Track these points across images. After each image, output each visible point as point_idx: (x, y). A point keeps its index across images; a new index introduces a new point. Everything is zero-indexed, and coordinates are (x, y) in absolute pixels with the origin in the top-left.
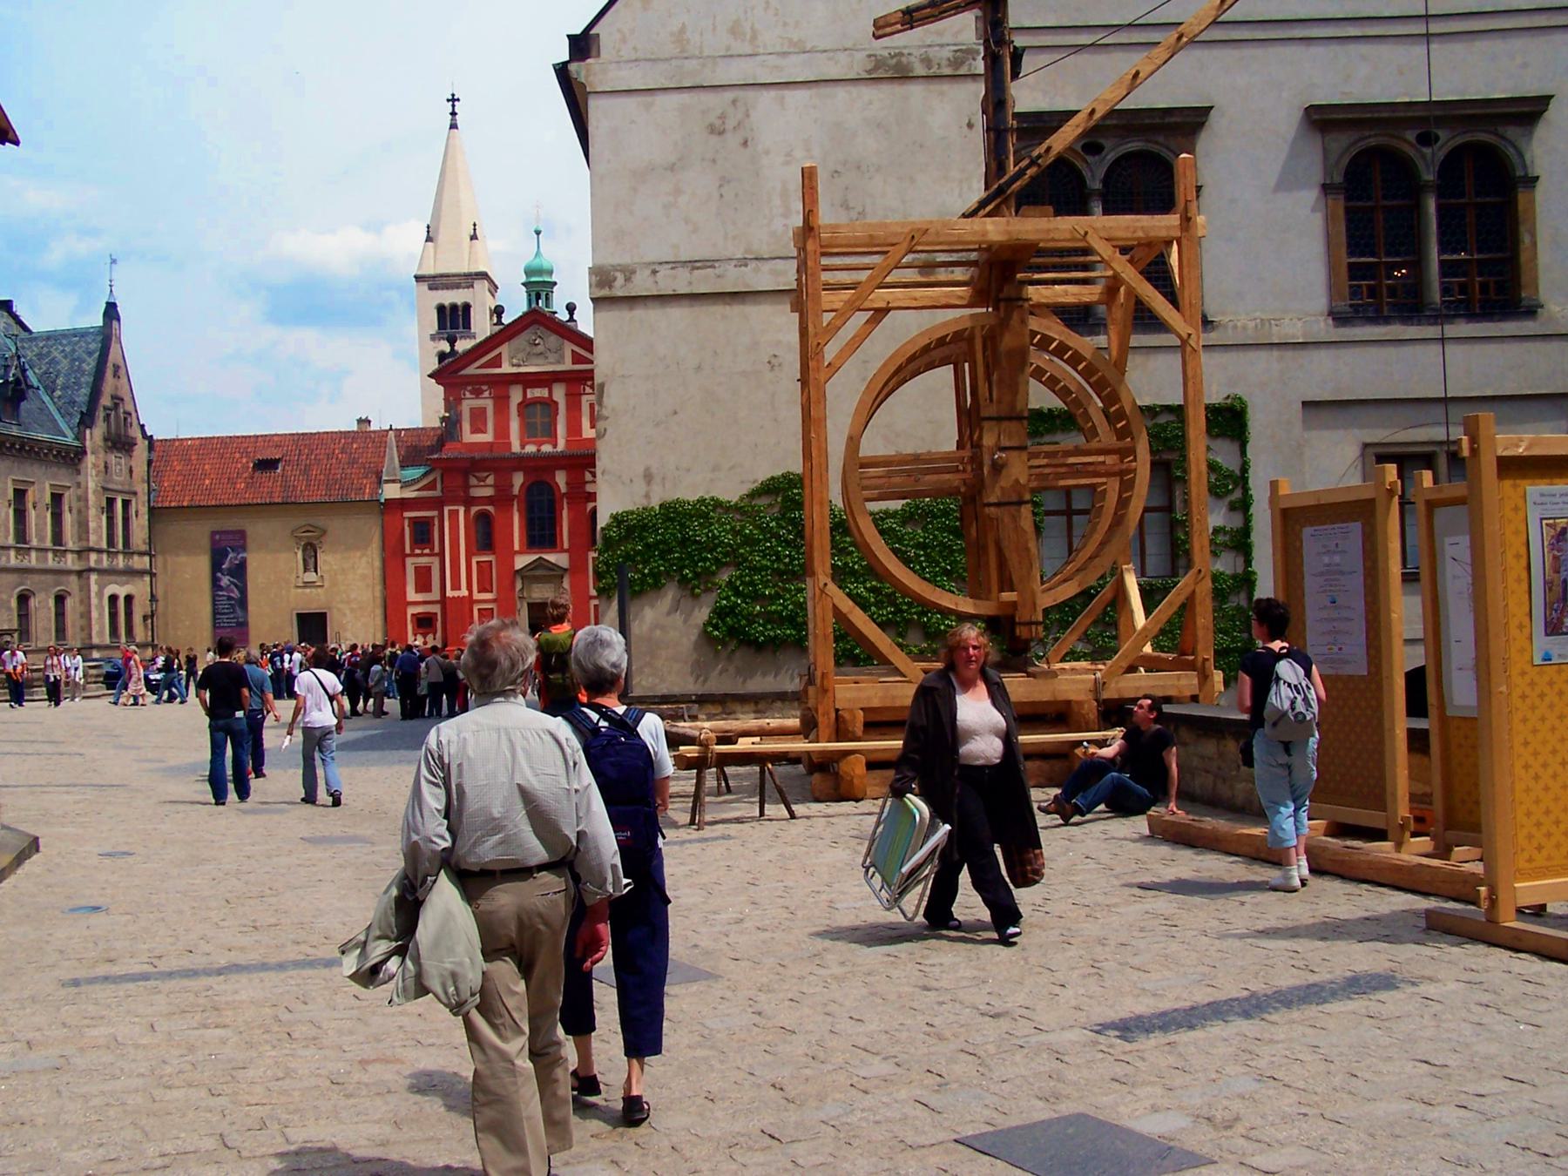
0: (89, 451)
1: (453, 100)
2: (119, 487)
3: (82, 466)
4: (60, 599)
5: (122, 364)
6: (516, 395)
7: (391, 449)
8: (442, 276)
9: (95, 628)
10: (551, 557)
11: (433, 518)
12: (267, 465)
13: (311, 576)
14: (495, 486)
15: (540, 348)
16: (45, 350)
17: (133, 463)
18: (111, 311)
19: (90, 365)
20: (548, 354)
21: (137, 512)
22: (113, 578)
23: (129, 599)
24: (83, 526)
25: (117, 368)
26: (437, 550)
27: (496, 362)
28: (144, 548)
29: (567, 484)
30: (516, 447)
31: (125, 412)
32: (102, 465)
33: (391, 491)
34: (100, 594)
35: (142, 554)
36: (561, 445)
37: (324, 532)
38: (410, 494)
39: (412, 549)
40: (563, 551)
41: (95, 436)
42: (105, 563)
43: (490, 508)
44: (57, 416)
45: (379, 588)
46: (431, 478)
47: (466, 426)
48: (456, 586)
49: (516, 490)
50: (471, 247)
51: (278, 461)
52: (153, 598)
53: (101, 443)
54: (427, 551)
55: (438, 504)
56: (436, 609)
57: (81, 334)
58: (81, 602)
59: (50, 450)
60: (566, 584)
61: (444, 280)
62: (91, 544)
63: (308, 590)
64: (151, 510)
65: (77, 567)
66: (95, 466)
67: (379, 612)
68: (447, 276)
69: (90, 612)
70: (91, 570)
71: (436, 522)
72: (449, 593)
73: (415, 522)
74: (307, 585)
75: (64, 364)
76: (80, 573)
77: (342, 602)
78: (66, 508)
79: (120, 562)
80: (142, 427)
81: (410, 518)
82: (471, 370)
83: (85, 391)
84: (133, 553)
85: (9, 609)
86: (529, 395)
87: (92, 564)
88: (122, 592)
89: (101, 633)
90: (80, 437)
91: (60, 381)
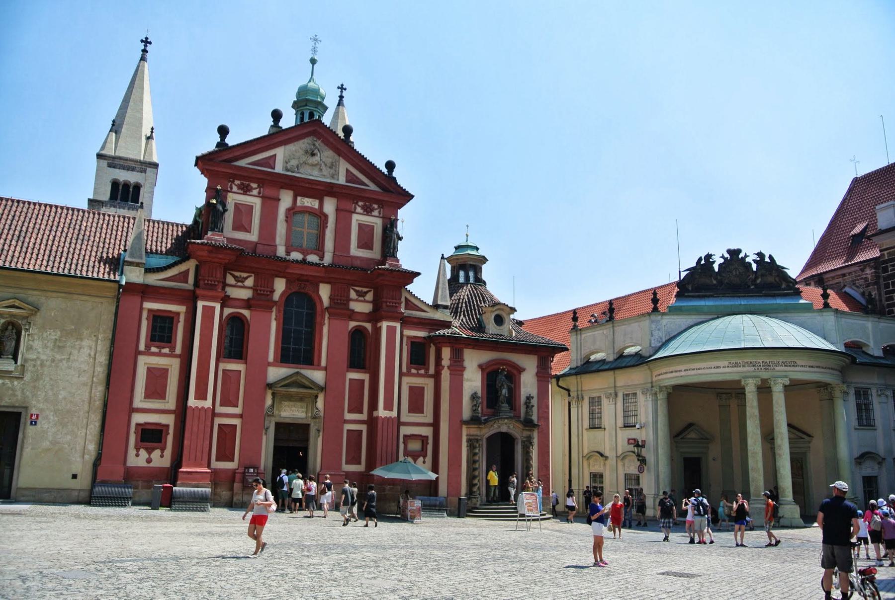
1: (146, 42)
6: (286, 199)
8: (120, 158)
11: (178, 314)
14: (254, 289)
20: (323, 167)
26: (178, 350)
29: (331, 298)
37: (36, 309)
38: (153, 279)
39: (148, 347)
40: (318, 367)
43: (246, 313)
46: (182, 268)
47: (229, 217)
48: (201, 395)
49: (276, 296)
50: (147, 144)
56: (169, 420)
60: (320, 403)
61: (122, 162)
68: (126, 160)
71: (182, 318)
72: (192, 402)
77: (46, 400)
81: (150, 311)
82: (243, 163)
86: (299, 203)
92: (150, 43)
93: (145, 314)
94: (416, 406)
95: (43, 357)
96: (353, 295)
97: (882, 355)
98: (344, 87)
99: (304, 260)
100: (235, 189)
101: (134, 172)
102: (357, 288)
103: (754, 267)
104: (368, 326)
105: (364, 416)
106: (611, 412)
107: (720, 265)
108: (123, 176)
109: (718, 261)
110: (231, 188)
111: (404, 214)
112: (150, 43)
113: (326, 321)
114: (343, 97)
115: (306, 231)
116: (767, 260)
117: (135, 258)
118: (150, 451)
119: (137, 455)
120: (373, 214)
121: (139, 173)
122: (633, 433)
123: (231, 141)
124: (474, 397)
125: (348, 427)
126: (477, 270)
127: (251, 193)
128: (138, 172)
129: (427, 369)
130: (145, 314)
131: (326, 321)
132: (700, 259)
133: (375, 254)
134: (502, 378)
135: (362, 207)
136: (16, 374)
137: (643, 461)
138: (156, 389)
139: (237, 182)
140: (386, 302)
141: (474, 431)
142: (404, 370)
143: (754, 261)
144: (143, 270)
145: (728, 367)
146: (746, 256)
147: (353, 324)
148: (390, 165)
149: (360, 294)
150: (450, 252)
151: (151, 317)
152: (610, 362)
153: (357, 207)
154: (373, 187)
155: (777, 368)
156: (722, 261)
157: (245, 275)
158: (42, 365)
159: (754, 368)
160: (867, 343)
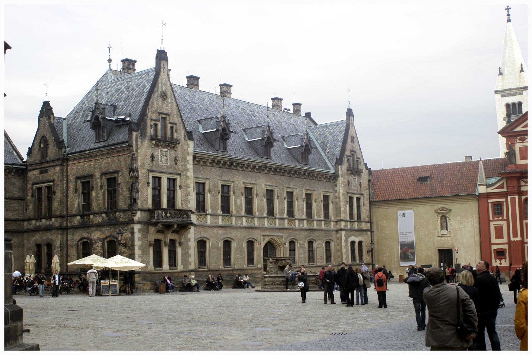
0: (340, 176)
1: (508, 9)
2: (355, 192)
3: (337, 183)
4: (328, 243)
5: (355, 136)
7: (481, 169)
8: (507, 90)
9: (344, 257)
11: (503, 202)
12: (423, 179)
13: (444, 232)
16: (323, 132)
17: (362, 181)
18: (349, 113)
19: (341, 137)
21: (364, 203)
22: (353, 233)
23: (360, 243)
24: (338, 209)
25: (352, 138)
26: (505, 218)
28: (367, 219)
31: (357, 158)
32: (347, 182)
33: (482, 190)
34: (346, 241)
35: (366, 222)
38: (490, 190)
39: (493, 218)
41: (343, 169)
42: (349, 227)
44: (327, 161)
45: (478, 237)
48: (515, 235)
51: (427, 177)
52: (372, 243)
53: (346, 172)
54: (500, 218)
55: (505, 195)
56: (506, 247)
57: (337, 124)
58: (338, 245)
59: (322, 176)
61: (508, 92)
62: (342, 218)
63: (443, 238)
64: (371, 202)
65: (335, 229)
66: (343, 182)
67: (478, 248)
69: (341, 249)
70: (342, 230)
71: (505, 203)
72: (512, 239)
73: (494, 204)
74: (443, 236)
75: (330, 138)
76: (337, 231)
77: (460, 244)
78: (330, 202)
79: (356, 226)
80: (366, 164)
81: (492, 203)
83: (339, 149)
84: (362, 222)
85: (304, 248)
87: (342, 227)
88: (357, 240)
89: (347, 259)
90: (337, 169)
91: (328, 146)
93: (490, 204)
95: (456, 227)
101: (517, 96)
108: (511, 100)
110: (516, 141)
118: (500, 260)
119: (496, 262)
121: (519, 96)
128: (518, 95)
130: (490, 204)
138: (499, 234)
139: (518, 138)
144: (485, 187)
158: (456, 231)
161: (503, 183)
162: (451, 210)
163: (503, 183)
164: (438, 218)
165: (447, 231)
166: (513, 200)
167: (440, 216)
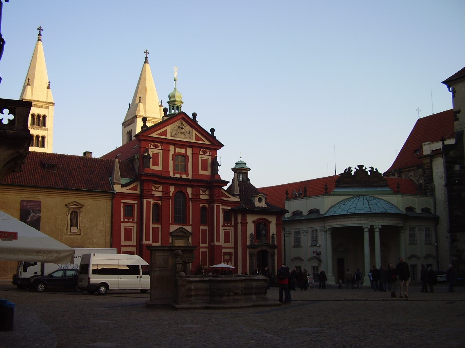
7: (117, 167)
10: (185, 227)
13: (74, 229)
15: (183, 131)
27: (165, 133)
30: (172, 175)
33: (118, 188)
36: (190, 177)
39: (124, 219)
40: (189, 225)
43: (159, 202)
46: (135, 184)
48: (148, 239)
54: (131, 220)
60: (190, 240)
63: (72, 237)
71: (136, 205)
72: (145, 242)
74: (72, 233)
92: (42, 30)
94: (227, 240)
95: (87, 225)
96: (201, 192)
97: (421, 213)
98: (148, 52)
99: (181, 177)
100: (152, 147)
102: (202, 189)
103: (369, 173)
104: (207, 205)
105: (207, 245)
106: (306, 239)
107: (354, 172)
109: (354, 171)
110: (150, 146)
111: (220, 153)
112: (42, 30)
113: (191, 204)
114: (147, 58)
115: (180, 164)
116: (375, 170)
117: (117, 181)
120: (207, 154)
122: (315, 249)
123: (149, 124)
124: (251, 235)
125: (201, 250)
126: (247, 174)
127: (158, 148)
129: (231, 223)
131: (191, 204)
132: (346, 170)
133: (207, 173)
134: (262, 226)
135: (203, 152)
136: (78, 233)
137: (320, 261)
139: (152, 143)
140: (216, 195)
141: (252, 250)
142: (221, 224)
143: (369, 170)
145: (357, 220)
146: (366, 168)
147: (201, 205)
148: (213, 130)
149: (204, 191)
150: (233, 166)
151: (124, 206)
152: (305, 216)
153: (200, 151)
154: (207, 142)
155: (377, 221)
156: (355, 170)
157: (158, 186)
159: (367, 221)
160: (415, 207)
161: (137, 186)
162: (83, 206)
163: (137, 186)
164: (69, 214)
165: (78, 229)
166: (148, 203)
167: (71, 211)
